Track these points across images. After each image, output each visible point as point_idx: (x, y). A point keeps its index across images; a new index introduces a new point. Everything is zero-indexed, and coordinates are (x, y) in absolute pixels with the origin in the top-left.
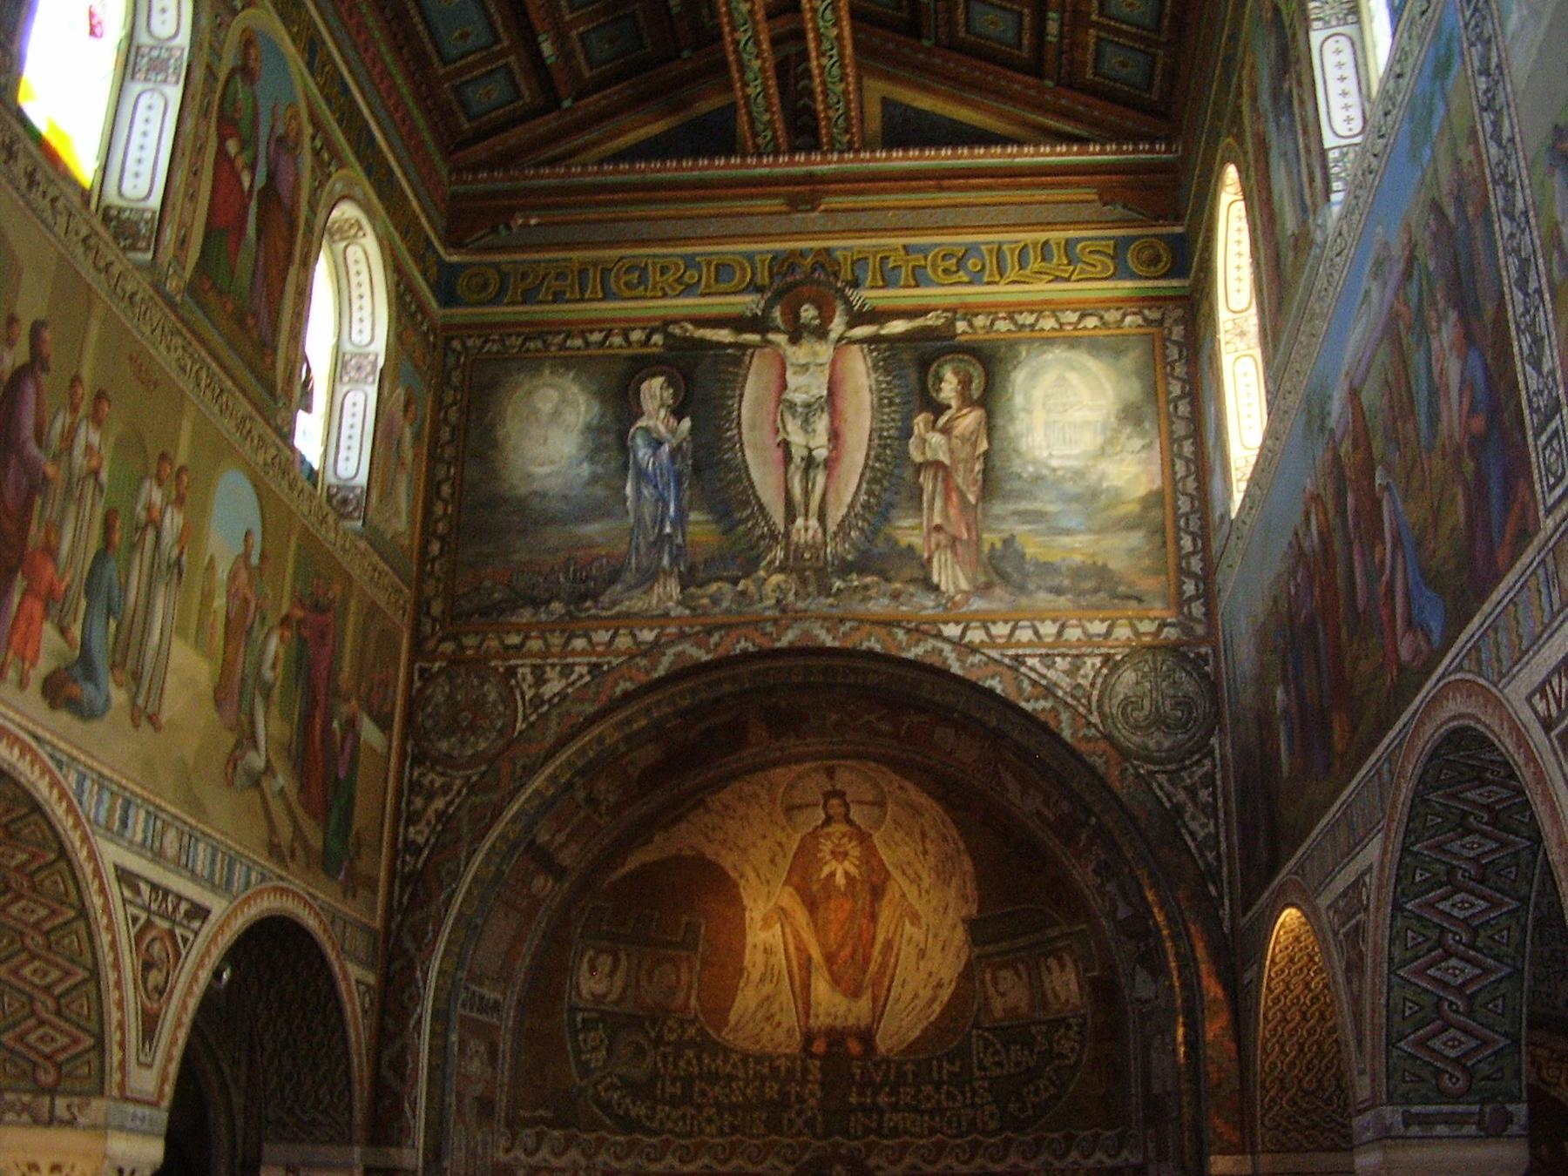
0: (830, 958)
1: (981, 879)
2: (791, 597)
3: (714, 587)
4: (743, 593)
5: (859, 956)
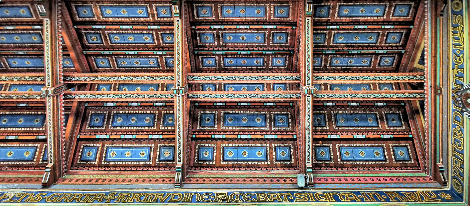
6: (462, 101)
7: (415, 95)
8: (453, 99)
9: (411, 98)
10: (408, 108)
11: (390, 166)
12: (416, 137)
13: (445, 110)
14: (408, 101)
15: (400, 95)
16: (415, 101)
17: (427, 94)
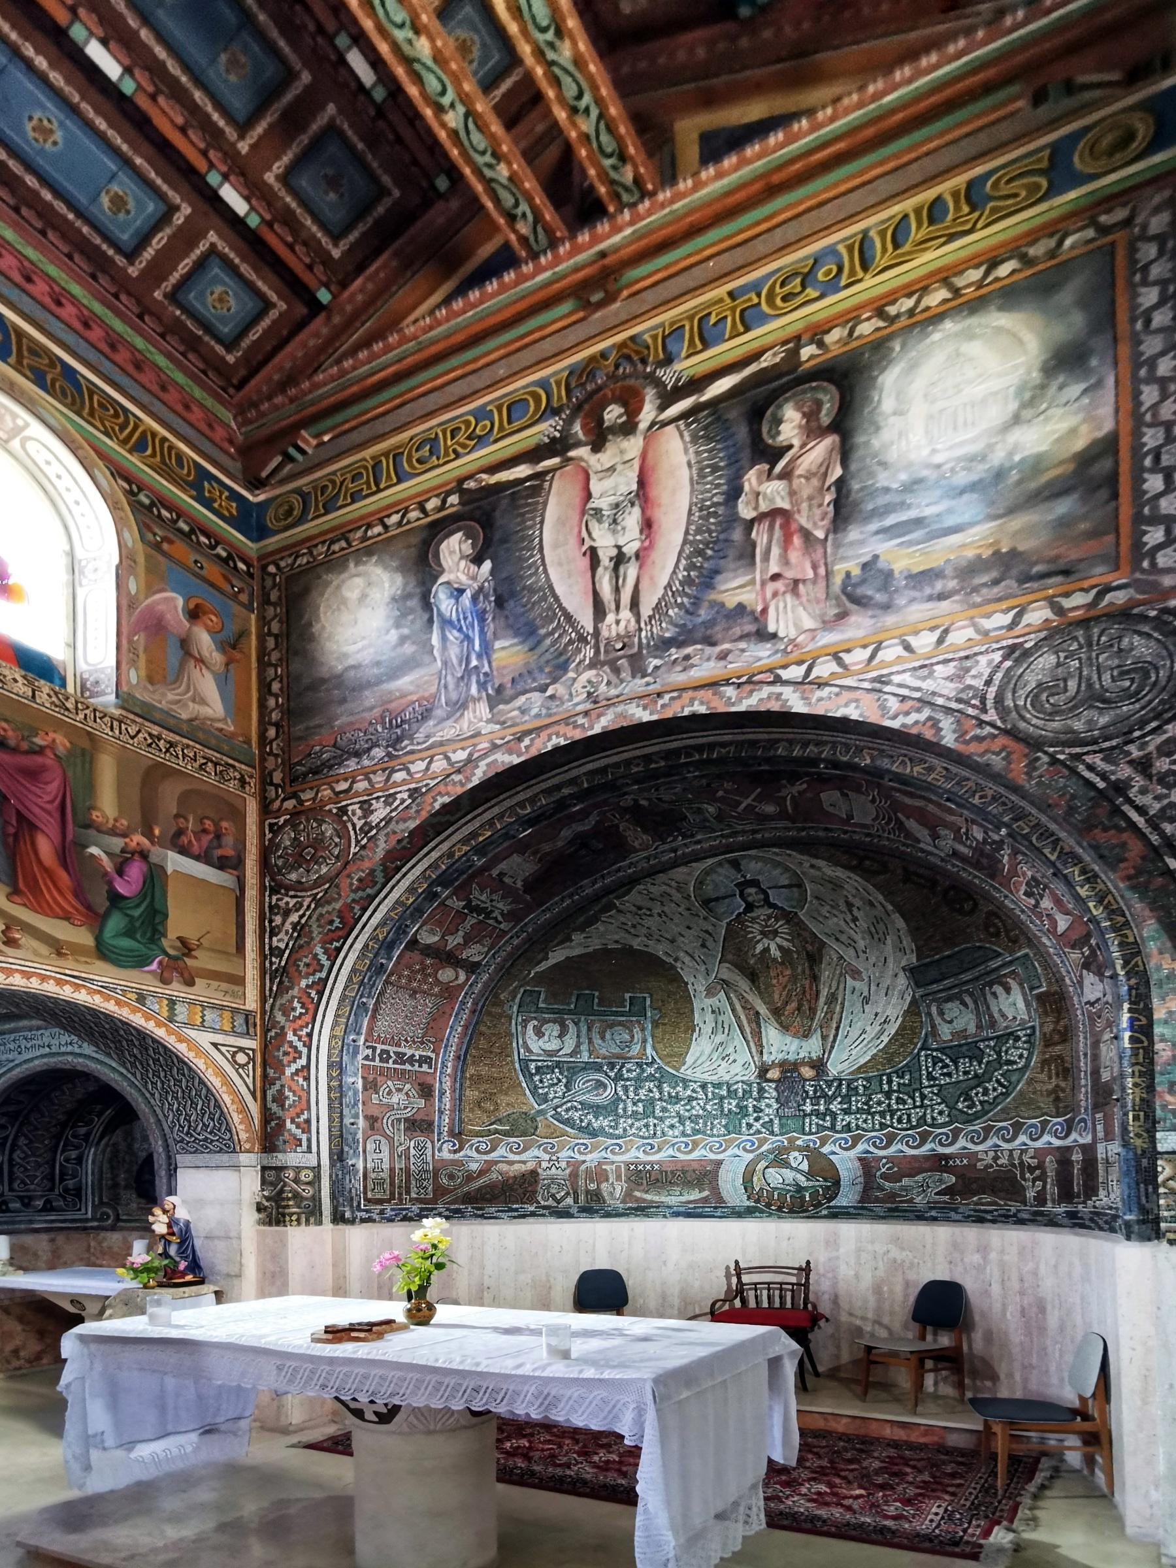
0: (777, 1012)
1: (915, 932)
2: (603, 688)
3: (523, 699)
4: (552, 697)
5: (806, 1007)
6: (599, 389)
7: (524, 207)
8: (592, 359)
9: (497, 200)
10: (438, 215)
11: (122, 284)
12: (337, 320)
13: (527, 357)
14: (475, 199)
15: (477, 138)
16: (496, 229)
17: (557, 260)
